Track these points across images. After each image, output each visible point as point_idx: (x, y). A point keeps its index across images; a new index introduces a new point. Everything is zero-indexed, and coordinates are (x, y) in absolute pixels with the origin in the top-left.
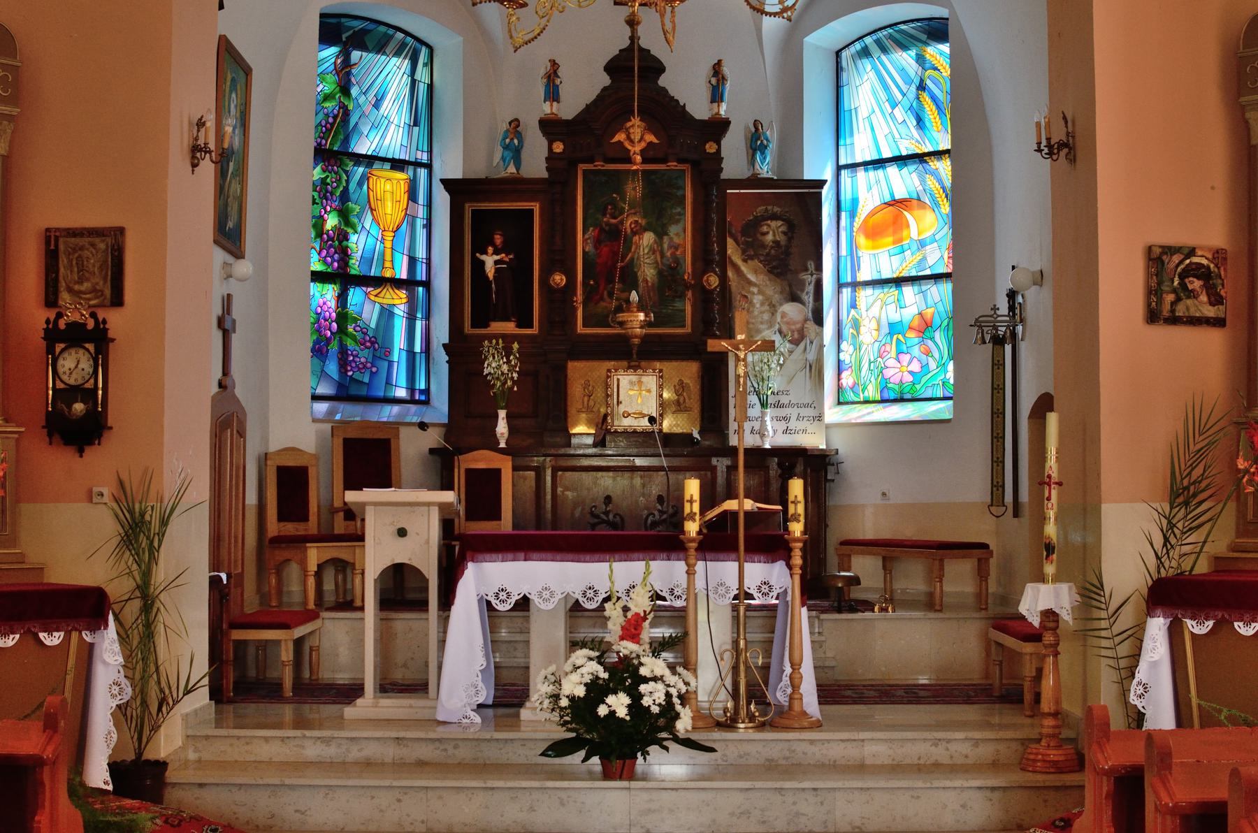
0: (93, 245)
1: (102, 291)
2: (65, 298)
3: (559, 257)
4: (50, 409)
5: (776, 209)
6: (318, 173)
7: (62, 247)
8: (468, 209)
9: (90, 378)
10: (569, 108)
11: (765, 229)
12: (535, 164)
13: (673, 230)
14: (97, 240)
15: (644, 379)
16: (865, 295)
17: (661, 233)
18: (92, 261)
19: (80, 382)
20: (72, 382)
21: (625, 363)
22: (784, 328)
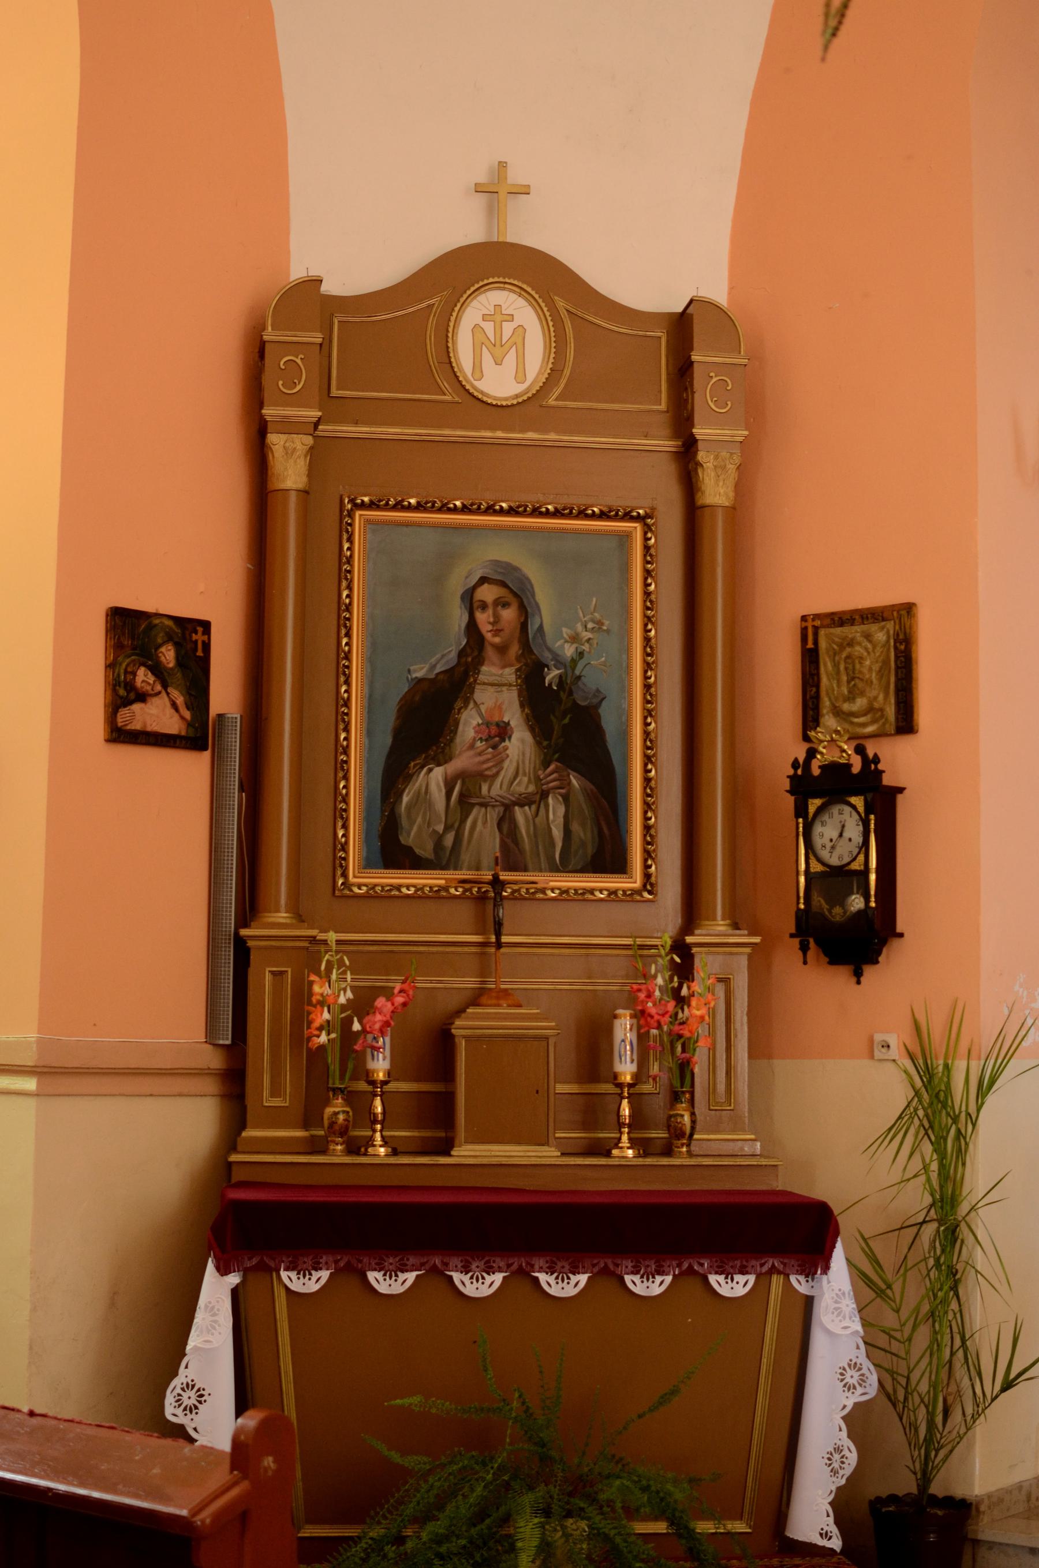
1: (882, 710)
4: (802, 906)
7: (823, 644)
9: (859, 853)
14: (873, 628)
18: (868, 663)
19: (846, 860)
20: (834, 861)
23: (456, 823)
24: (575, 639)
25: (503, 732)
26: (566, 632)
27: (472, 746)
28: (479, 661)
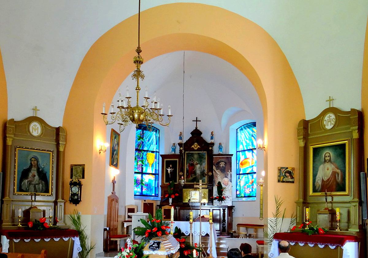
0: (79, 168)
2: (74, 177)
3: (182, 170)
5: (223, 160)
6: (137, 154)
7: (73, 168)
8: (165, 160)
10: (184, 141)
11: (220, 164)
12: (178, 152)
13: (203, 164)
15: (196, 192)
16: (241, 176)
17: (201, 165)
20: (74, 193)
21: (193, 189)
22: (224, 183)
23: (29, 187)
24: (43, 165)
25: (35, 176)
26: (42, 164)
27: (31, 177)
28: (32, 168)
